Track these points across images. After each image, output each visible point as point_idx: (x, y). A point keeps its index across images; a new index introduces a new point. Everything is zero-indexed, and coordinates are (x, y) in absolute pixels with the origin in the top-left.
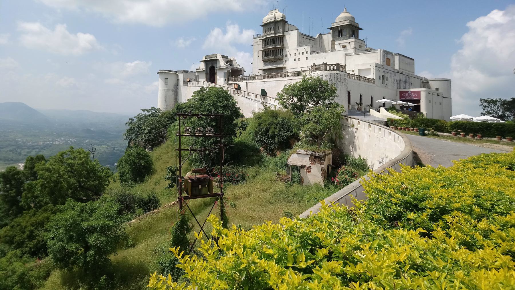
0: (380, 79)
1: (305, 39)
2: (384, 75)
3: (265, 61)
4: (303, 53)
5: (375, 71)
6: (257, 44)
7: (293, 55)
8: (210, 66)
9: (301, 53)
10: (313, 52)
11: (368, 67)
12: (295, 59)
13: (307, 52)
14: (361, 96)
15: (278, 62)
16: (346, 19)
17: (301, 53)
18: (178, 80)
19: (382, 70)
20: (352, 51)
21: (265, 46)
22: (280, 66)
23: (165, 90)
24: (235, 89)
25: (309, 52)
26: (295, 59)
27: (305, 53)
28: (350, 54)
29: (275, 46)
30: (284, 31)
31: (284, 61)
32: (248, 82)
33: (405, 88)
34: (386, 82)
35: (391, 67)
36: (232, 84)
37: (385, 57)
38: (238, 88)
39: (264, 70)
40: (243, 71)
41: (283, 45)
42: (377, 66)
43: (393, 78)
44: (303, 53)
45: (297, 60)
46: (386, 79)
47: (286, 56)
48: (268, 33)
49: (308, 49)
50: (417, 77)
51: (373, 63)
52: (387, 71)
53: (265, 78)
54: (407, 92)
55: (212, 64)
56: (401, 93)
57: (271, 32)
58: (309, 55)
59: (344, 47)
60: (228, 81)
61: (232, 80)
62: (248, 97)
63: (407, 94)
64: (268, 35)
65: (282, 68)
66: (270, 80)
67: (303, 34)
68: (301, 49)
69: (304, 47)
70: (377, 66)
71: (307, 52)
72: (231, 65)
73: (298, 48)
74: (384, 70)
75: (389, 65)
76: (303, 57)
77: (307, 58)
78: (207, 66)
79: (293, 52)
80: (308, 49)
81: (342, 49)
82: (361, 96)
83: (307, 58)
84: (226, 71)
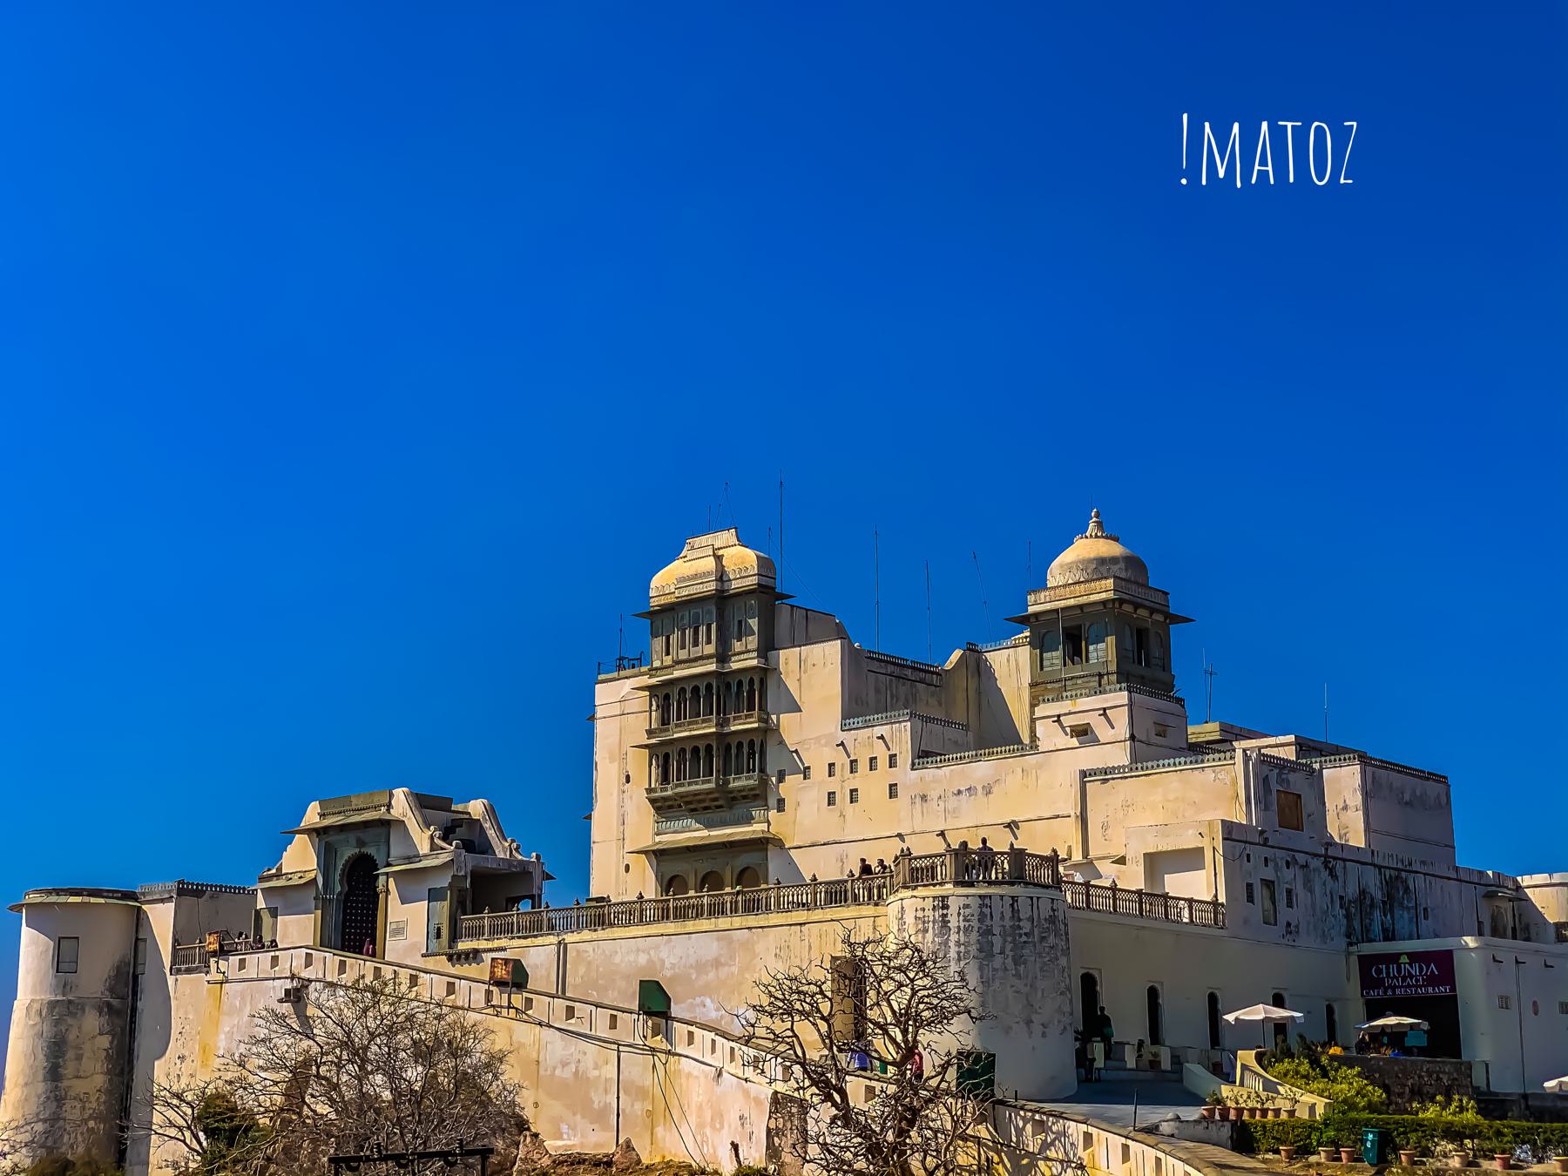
0: (1250, 899)
1: (877, 685)
2: (1269, 874)
3: (664, 808)
4: (873, 759)
5: (1220, 860)
6: (616, 710)
7: (819, 772)
8: (348, 852)
9: (863, 765)
10: (923, 756)
11: (1189, 841)
12: (831, 796)
13: (892, 758)
14: (1153, 994)
15: (739, 810)
16: (1101, 566)
17: (863, 765)
19: (1259, 852)
20: (1119, 756)
21: (665, 721)
22: (755, 829)
23: (52, 1005)
24: (500, 983)
25: (905, 758)
26: (831, 796)
27: (883, 762)
28: (1106, 774)
29: (722, 723)
30: (768, 647)
31: (772, 801)
32: (569, 938)
33: (1389, 935)
34: (1285, 914)
35: (1306, 833)
36: (476, 952)
37: (1275, 787)
38: (516, 978)
39: (659, 855)
40: (537, 876)
42: (1230, 831)
43: (1318, 889)
44: (873, 759)
45: (843, 797)
48: (683, 655)
49: (900, 734)
50: (1460, 878)
51: (1210, 823)
53: (665, 916)
54: (1394, 958)
55: (361, 843)
56: (1366, 962)
57: (696, 652)
58: (905, 775)
60: (454, 937)
61: (476, 933)
62: (572, 1025)
63: (1393, 969)
64: (678, 662)
65: (761, 844)
66: (690, 925)
67: (872, 657)
68: (868, 739)
69: (878, 731)
70: (1230, 831)
71: (892, 758)
72: (468, 846)
73: (847, 737)
74: (1268, 852)
75: (1299, 828)
76: (872, 785)
77: (893, 787)
78: (327, 856)
79: (816, 758)
80: (900, 734)
81: (1075, 742)
82: (1153, 994)
83: (893, 787)
84: (444, 881)
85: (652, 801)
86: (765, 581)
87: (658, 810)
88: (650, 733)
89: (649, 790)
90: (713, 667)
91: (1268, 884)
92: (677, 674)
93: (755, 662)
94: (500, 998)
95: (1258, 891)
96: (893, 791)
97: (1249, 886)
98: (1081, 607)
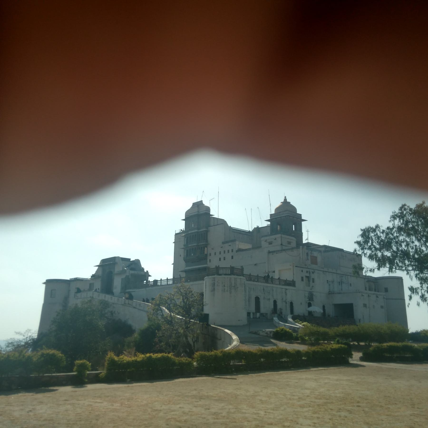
9: (226, 252)
12: (220, 259)
17: (226, 252)
18: (69, 291)
19: (305, 270)
21: (187, 243)
24: (127, 299)
26: (220, 259)
27: (230, 251)
31: (208, 260)
39: (185, 271)
41: (207, 241)
45: (222, 259)
46: (311, 281)
47: (210, 255)
52: (313, 270)
59: (270, 243)
84: (124, 276)
85: (184, 260)
86: (207, 212)
87: (186, 262)
88: (184, 245)
89: (184, 258)
90: (196, 231)
91: (307, 277)
92: (189, 232)
93: (205, 229)
94: (127, 301)
95: (304, 278)
96: (232, 257)
97: (302, 278)
98: (281, 217)
